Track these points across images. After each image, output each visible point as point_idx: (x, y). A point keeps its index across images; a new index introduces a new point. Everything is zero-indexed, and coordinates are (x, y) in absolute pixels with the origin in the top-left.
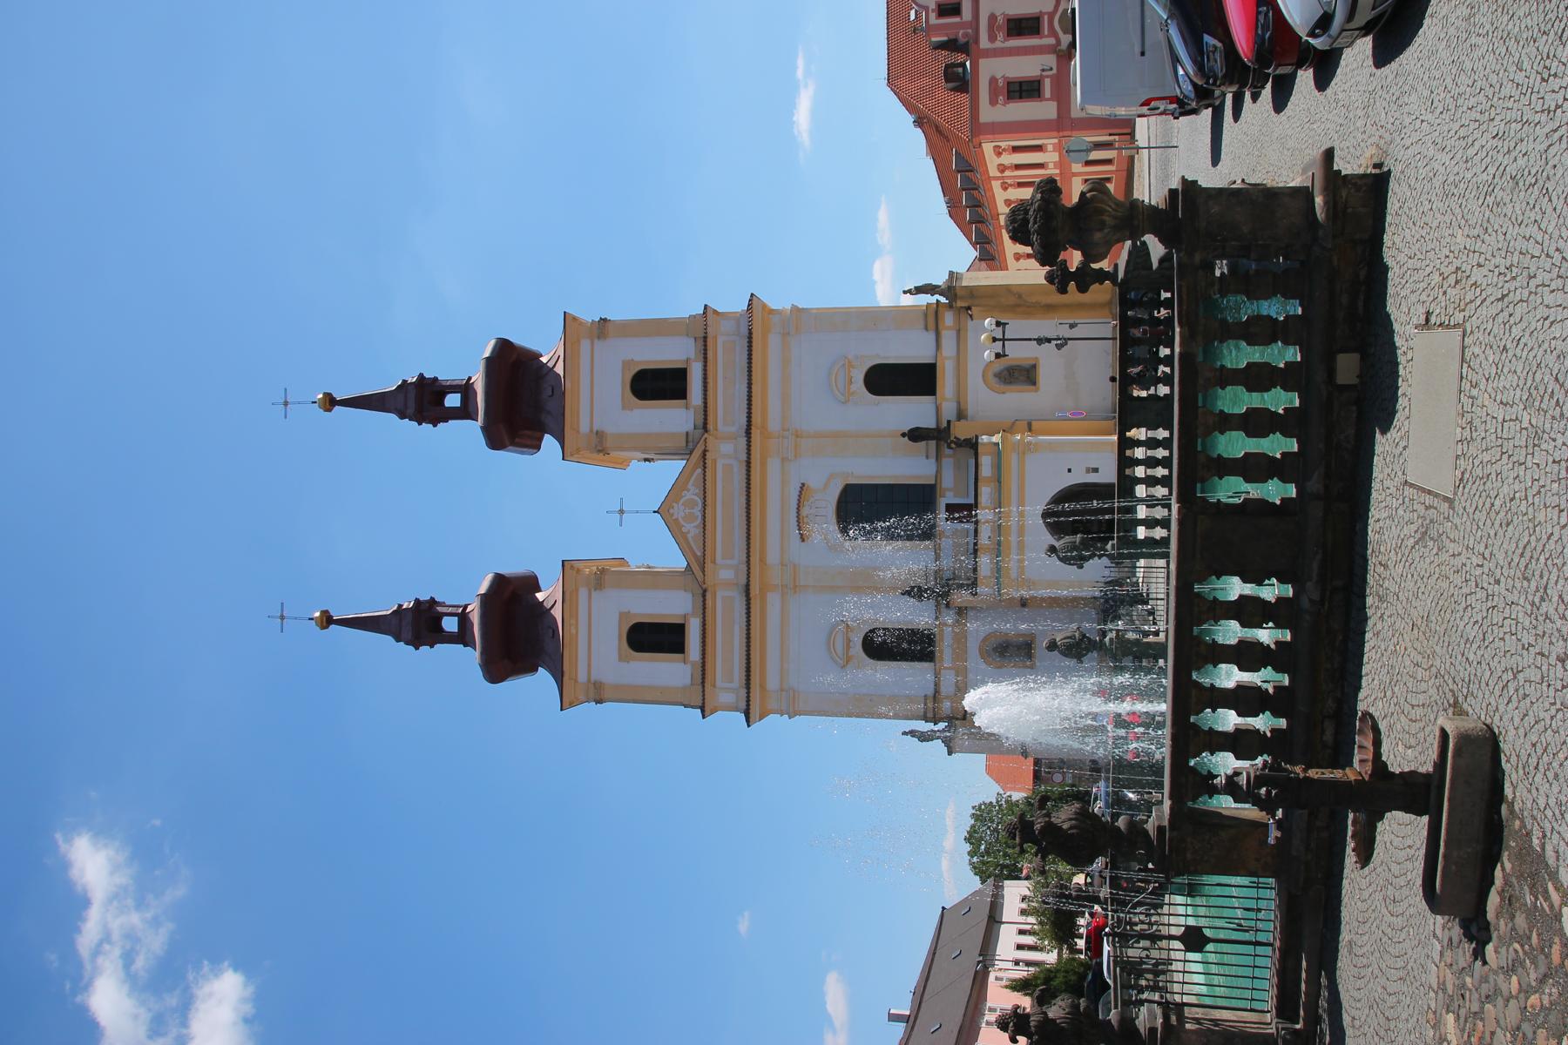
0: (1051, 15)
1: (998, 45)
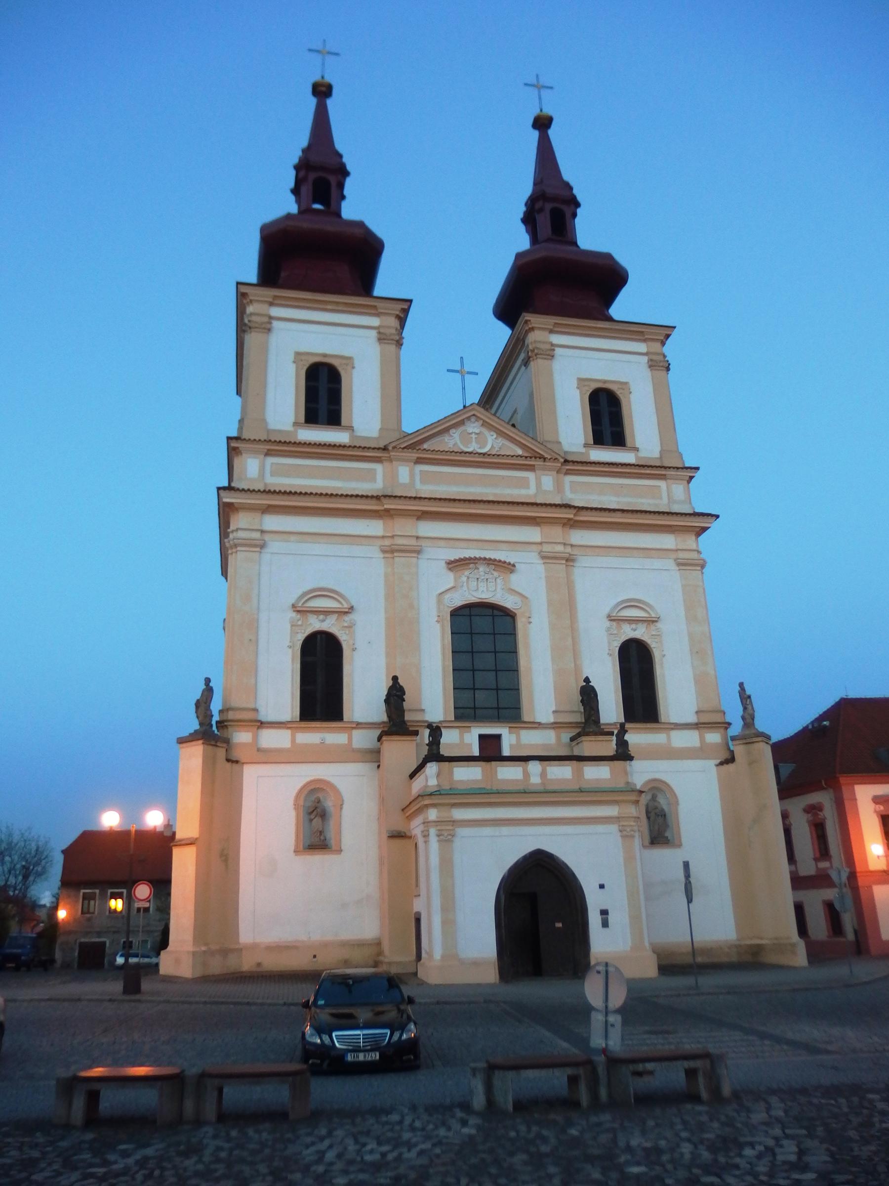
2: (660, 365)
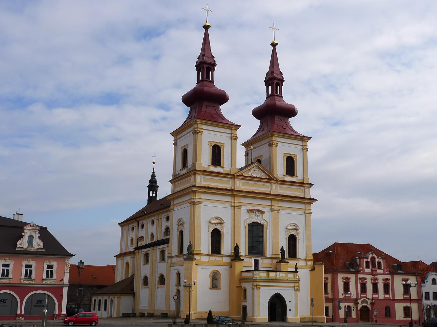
0: (366, 297)
1: (359, 280)
2: (305, 149)
